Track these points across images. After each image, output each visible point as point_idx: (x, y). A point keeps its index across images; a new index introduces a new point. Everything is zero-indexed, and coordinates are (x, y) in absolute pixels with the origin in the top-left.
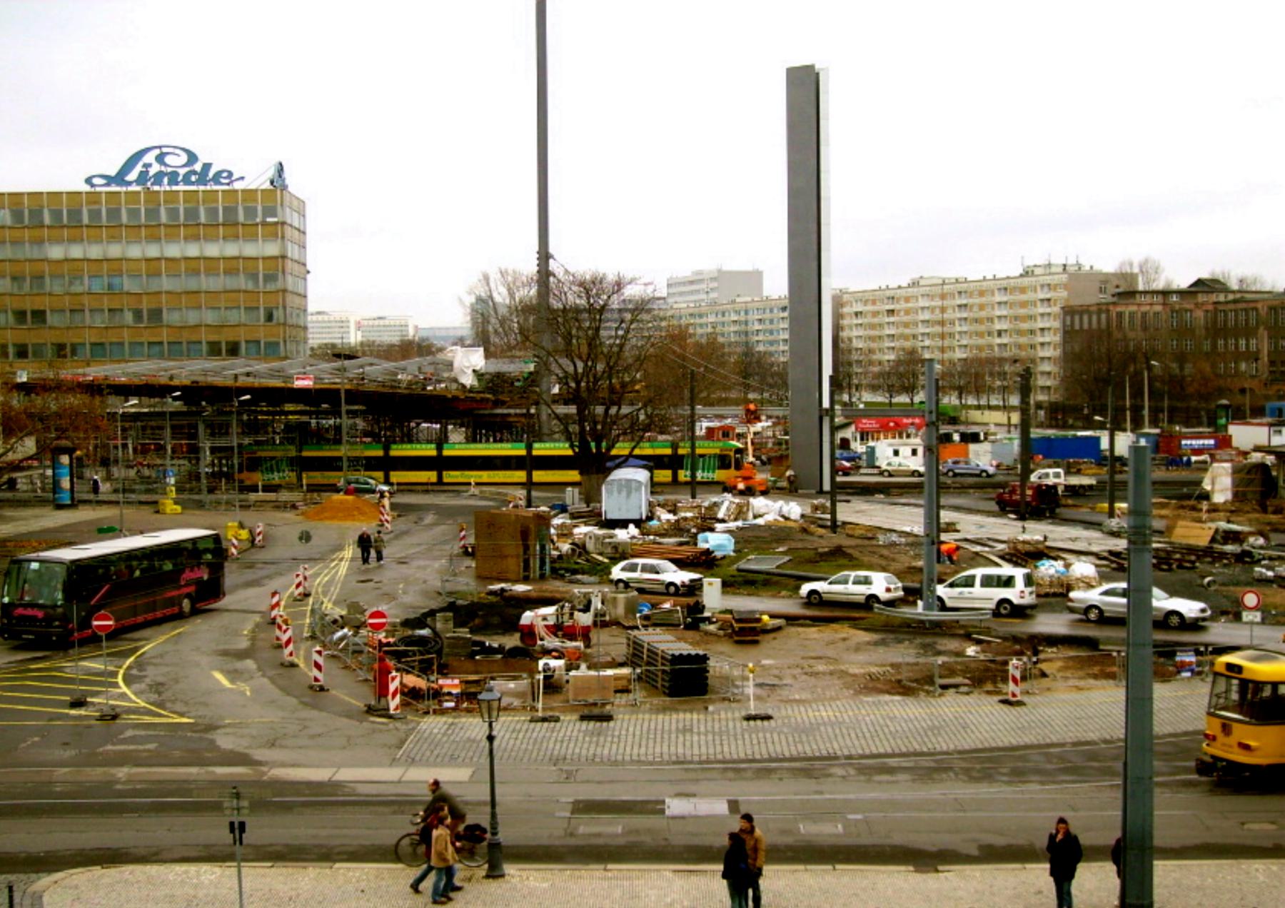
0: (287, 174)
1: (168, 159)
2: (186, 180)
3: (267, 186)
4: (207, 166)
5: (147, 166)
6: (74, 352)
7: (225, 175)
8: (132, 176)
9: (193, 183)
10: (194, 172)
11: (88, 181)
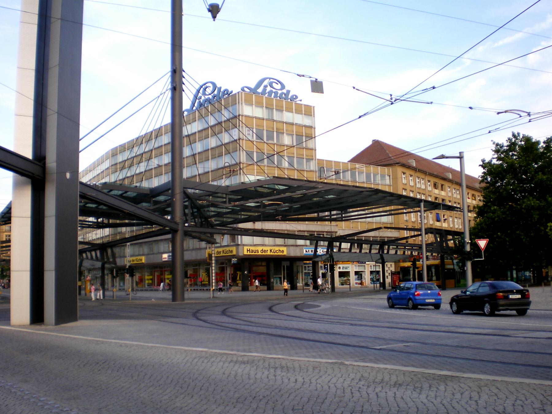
1: (274, 85)
4: (288, 92)
8: (260, 90)
10: (283, 93)
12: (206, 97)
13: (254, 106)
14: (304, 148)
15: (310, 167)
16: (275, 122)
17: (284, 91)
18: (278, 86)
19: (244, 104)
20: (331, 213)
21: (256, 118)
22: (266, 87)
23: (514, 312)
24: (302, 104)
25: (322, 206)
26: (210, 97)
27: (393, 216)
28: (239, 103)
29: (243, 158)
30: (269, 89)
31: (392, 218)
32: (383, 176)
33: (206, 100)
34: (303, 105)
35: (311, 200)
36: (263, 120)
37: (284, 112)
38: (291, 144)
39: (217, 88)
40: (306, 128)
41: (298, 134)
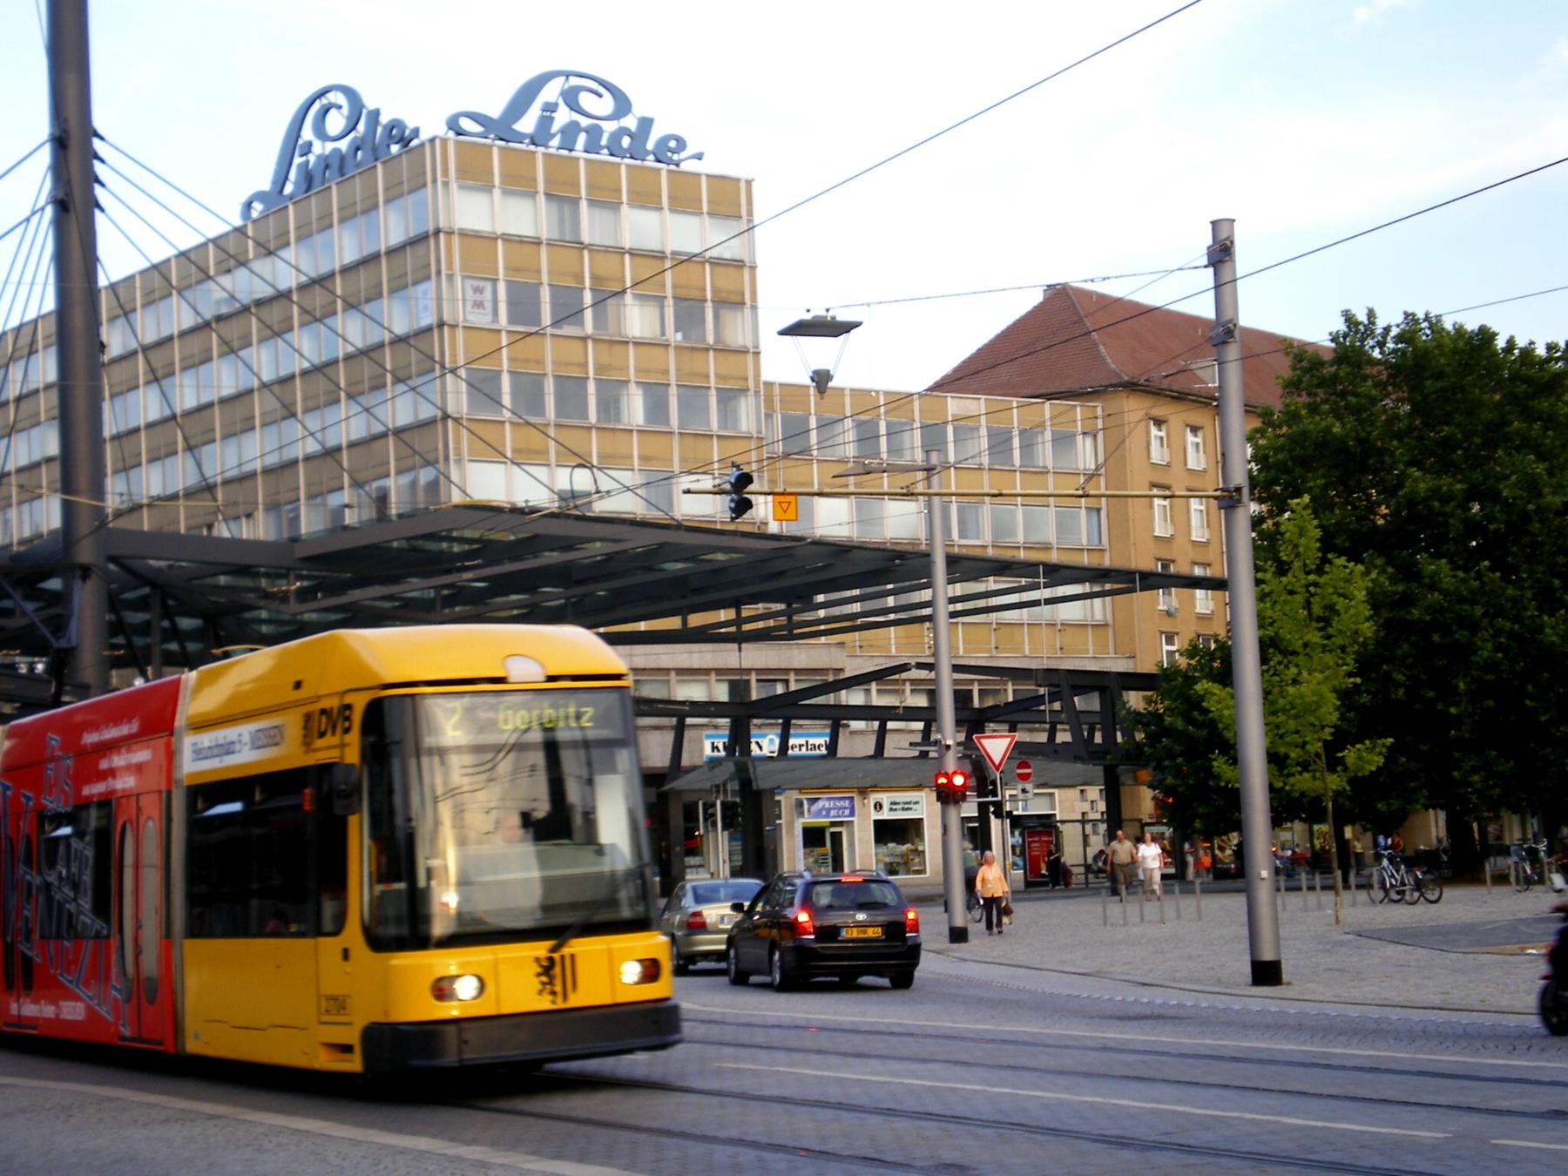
1: (586, 100)
4: (646, 124)
10: (624, 131)
12: (330, 146)
13: (497, 192)
14: (707, 350)
15: (736, 420)
16: (586, 253)
17: (630, 122)
18: (605, 105)
19: (454, 186)
20: (738, 613)
21: (507, 238)
22: (550, 108)
23: (885, 982)
24: (698, 175)
25: (695, 591)
26: (343, 145)
27: (1108, 599)
28: (434, 181)
29: (458, 397)
30: (563, 116)
31: (1104, 605)
32: (1063, 440)
33: (325, 163)
34: (704, 179)
35: (649, 569)
36: (534, 247)
37: (625, 208)
38: (658, 332)
39: (364, 112)
40: (719, 269)
41: (683, 293)
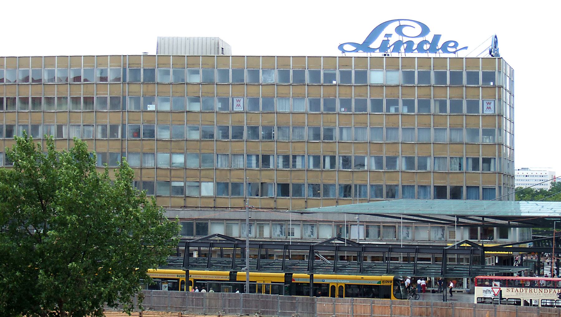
0: (499, 46)
1: (405, 31)
2: (420, 48)
3: (487, 55)
4: (437, 38)
5: (388, 35)
6: (326, 193)
7: (452, 44)
8: (376, 44)
9: (425, 51)
10: (426, 42)
11: (341, 47)
17: (429, 37)
